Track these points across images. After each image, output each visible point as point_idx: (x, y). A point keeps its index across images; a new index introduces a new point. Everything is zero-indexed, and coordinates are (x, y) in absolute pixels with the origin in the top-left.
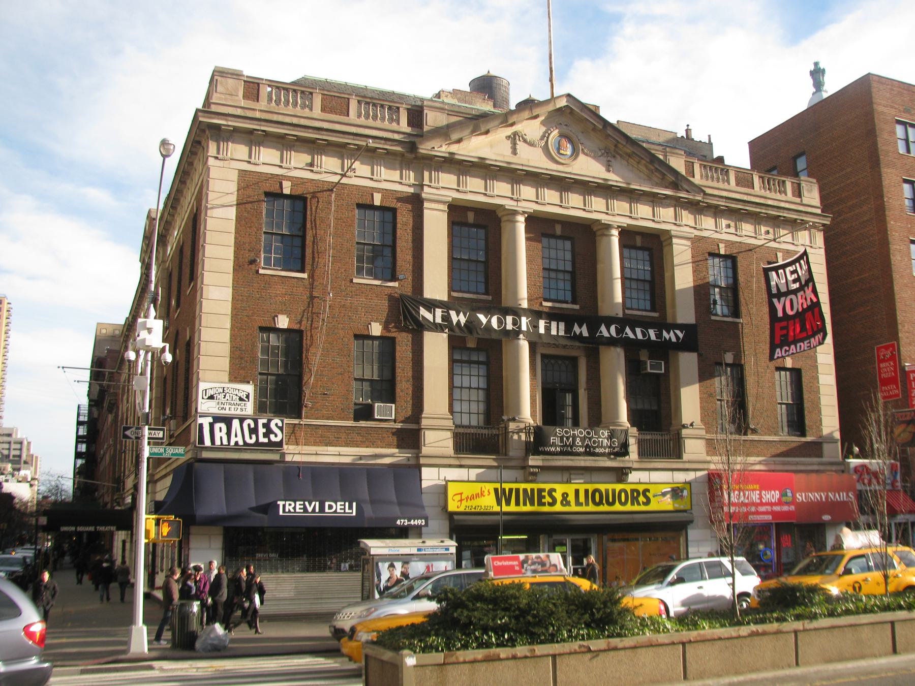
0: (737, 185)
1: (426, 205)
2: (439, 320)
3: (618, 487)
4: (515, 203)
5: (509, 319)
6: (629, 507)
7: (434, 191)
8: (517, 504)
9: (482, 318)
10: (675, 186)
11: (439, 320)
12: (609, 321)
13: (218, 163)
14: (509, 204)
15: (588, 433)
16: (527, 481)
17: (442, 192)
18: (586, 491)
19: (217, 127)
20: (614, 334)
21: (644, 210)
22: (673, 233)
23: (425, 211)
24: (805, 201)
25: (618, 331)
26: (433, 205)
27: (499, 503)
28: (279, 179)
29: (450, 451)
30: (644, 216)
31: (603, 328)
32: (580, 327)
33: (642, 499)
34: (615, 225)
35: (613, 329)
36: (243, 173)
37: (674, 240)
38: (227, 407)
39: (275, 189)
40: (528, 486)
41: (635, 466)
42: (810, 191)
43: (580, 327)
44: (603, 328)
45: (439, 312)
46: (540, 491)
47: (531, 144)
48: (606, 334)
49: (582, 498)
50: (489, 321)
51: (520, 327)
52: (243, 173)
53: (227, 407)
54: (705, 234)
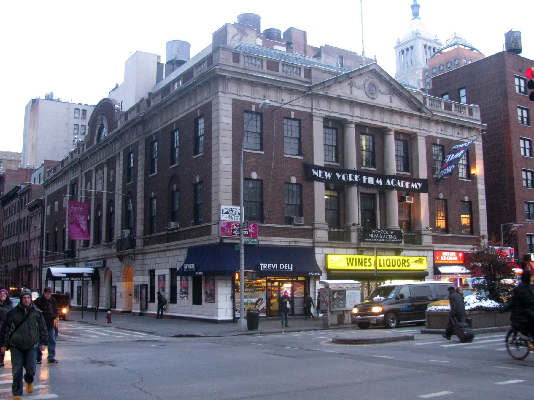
0: (445, 109)
1: (314, 118)
2: (320, 176)
3: (397, 258)
4: (351, 118)
5: (350, 175)
6: (401, 268)
7: (317, 111)
8: (356, 265)
9: (338, 175)
10: (419, 110)
11: (320, 176)
12: (391, 177)
13: (224, 95)
14: (349, 118)
15: (385, 232)
16: (359, 254)
17: (321, 112)
18: (384, 260)
19: (224, 77)
20: (393, 184)
21: (406, 121)
22: (418, 134)
23: (314, 121)
24: (474, 117)
25: (395, 183)
26: (317, 119)
27: (348, 265)
28: (251, 103)
29: (327, 239)
30: (407, 125)
31: (388, 181)
32: (379, 180)
33: (406, 264)
34: (393, 129)
35: (392, 181)
36: (234, 100)
37: (419, 137)
38: (233, 217)
39: (248, 109)
40: (360, 257)
41: (403, 248)
42: (476, 112)
43: (379, 180)
44: (388, 181)
45: (320, 172)
46: (365, 259)
47: (358, 88)
48: (389, 184)
49: (382, 264)
50: (341, 177)
51: (355, 180)
52: (234, 100)
53: (233, 217)
54: (432, 134)
